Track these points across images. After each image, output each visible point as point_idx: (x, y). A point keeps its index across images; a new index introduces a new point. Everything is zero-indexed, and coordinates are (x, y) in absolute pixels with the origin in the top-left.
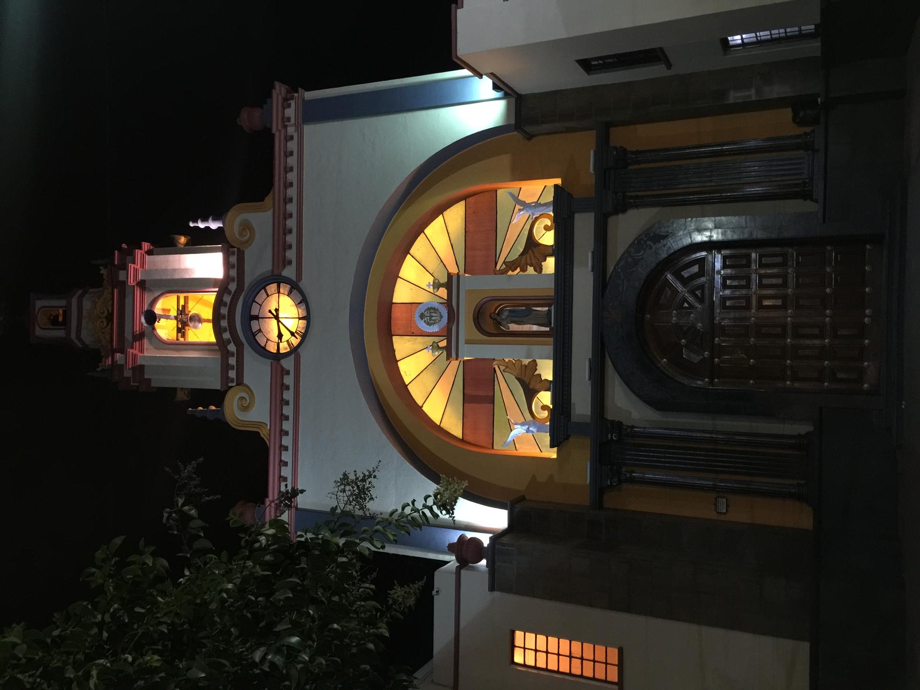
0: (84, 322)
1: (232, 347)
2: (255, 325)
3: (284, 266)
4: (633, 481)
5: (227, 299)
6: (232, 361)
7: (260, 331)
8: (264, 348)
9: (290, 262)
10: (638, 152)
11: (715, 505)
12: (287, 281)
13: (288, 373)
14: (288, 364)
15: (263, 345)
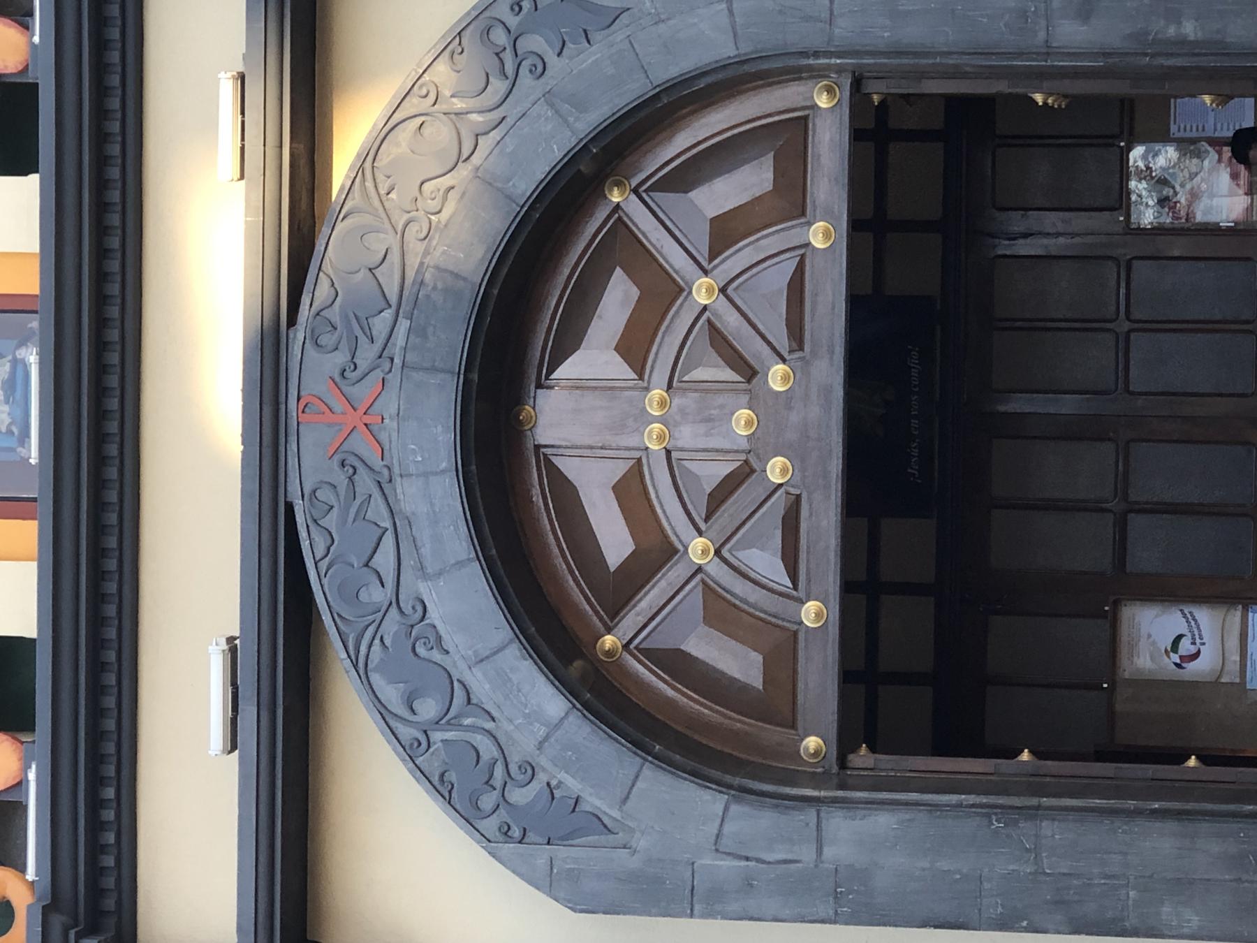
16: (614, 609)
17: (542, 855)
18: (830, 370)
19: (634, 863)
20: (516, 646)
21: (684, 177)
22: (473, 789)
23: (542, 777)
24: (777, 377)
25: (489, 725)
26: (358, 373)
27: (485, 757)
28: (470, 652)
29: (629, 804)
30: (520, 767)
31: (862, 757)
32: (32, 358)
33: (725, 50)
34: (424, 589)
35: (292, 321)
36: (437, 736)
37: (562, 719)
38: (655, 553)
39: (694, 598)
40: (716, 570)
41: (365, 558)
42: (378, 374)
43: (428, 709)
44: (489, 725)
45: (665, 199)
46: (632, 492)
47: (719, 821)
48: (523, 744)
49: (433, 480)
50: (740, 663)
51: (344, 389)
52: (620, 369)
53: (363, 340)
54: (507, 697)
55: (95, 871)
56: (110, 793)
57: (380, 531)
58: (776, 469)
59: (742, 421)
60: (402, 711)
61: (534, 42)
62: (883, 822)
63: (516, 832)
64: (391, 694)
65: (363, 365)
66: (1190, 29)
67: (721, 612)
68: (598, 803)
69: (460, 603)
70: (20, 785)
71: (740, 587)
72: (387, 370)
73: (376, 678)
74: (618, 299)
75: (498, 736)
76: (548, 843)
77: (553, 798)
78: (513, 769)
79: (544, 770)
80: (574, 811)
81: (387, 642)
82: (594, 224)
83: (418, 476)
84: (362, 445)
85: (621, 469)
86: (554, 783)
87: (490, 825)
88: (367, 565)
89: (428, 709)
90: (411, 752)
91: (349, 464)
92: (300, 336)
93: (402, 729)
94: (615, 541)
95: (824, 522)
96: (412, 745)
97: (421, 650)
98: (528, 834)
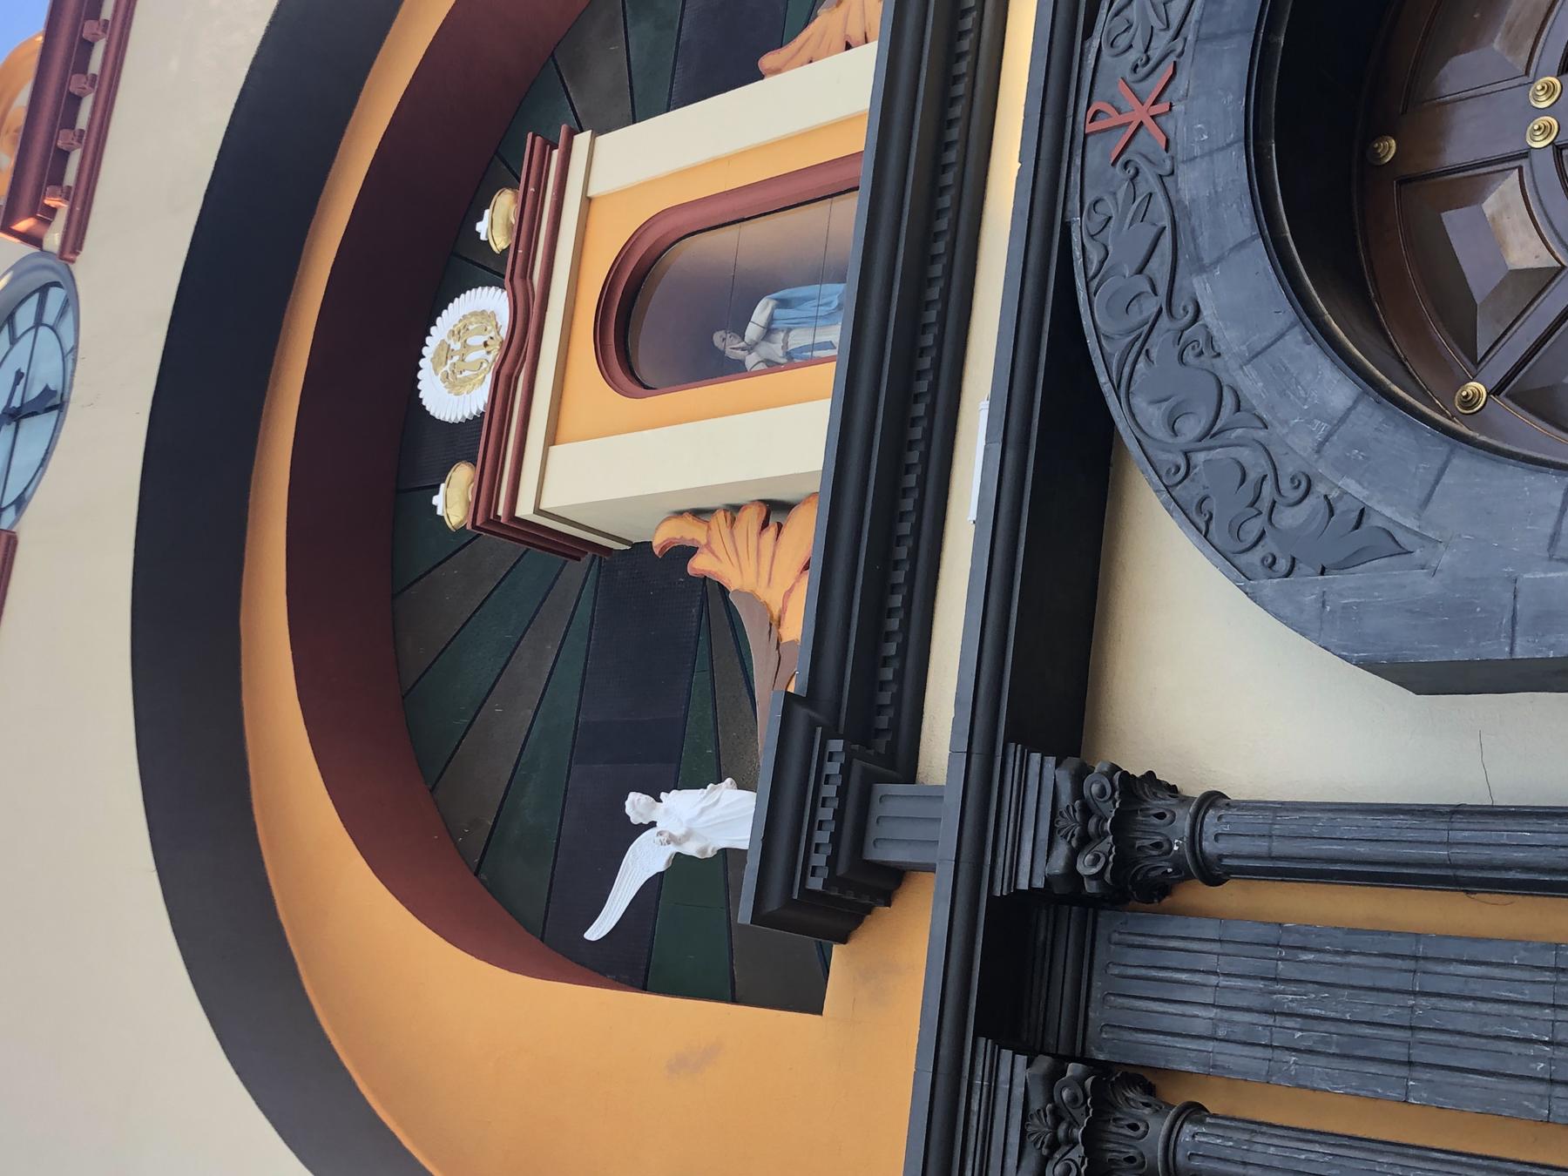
17: (1309, 589)
19: (1428, 586)
20: (1297, 335)
23: (1320, 489)
25: (1261, 434)
26: (1151, 63)
27: (1253, 476)
28: (1244, 348)
29: (1432, 506)
30: (1292, 480)
34: (1200, 287)
35: (1088, 34)
36: (1199, 458)
37: (1350, 410)
41: (1136, 266)
42: (1172, 58)
43: (1191, 428)
44: (1261, 434)
47: (1555, 515)
48: (1298, 444)
49: (1218, 157)
51: (1137, 87)
53: (1158, 25)
54: (1283, 394)
56: (897, 601)
57: (1155, 230)
60: (1161, 433)
63: (1283, 565)
64: (1152, 416)
65: (1155, 54)
68: (1388, 512)
69: (1238, 291)
72: (1179, 50)
73: (1139, 402)
75: (1271, 449)
76: (1322, 573)
77: (1332, 513)
78: (1285, 485)
79: (1322, 478)
80: (1357, 526)
81: (1154, 354)
83: (1202, 156)
86: (1334, 495)
87: (1255, 557)
88: (1140, 271)
92: (1096, 43)
93: (1160, 456)
96: (1168, 471)
97: (1189, 355)
98: (1298, 565)
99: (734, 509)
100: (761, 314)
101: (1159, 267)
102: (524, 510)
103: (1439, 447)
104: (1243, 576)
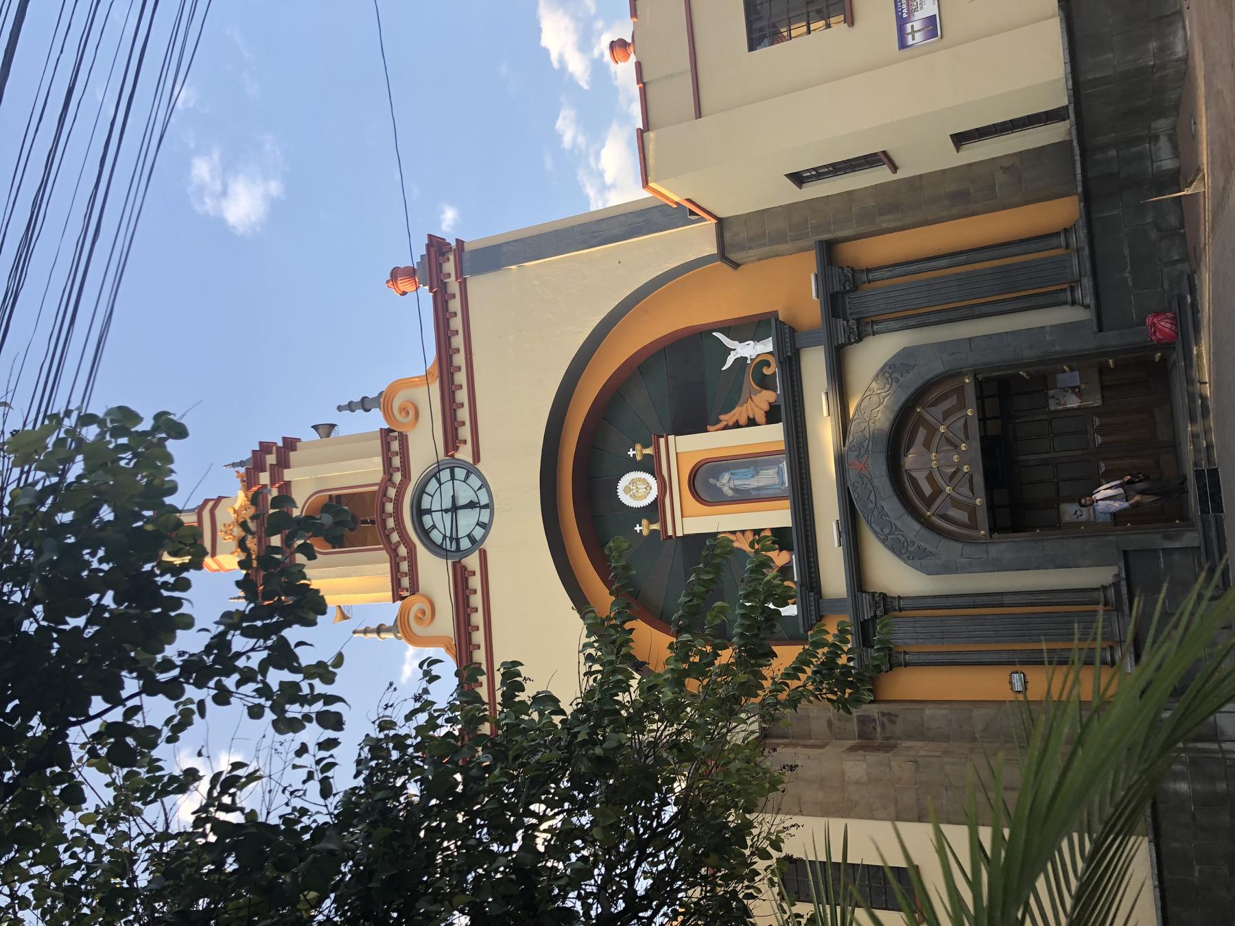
0: (220, 535)
1: (403, 551)
2: (427, 520)
3: (456, 449)
4: (906, 665)
5: (392, 492)
6: (404, 566)
7: (434, 527)
8: (440, 547)
9: (465, 442)
10: (868, 270)
11: (1011, 682)
12: (462, 464)
13: (474, 573)
14: (472, 562)
15: (439, 543)
16: (929, 506)
18: (977, 444)
21: (935, 404)
22: (900, 549)
24: (963, 447)
31: (996, 535)
32: (784, 465)
33: (942, 369)
38: (938, 491)
39: (948, 500)
40: (954, 494)
43: (887, 531)
45: (932, 409)
46: (930, 478)
50: (962, 516)
52: (925, 450)
55: (811, 578)
58: (965, 469)
59: (956, 458)
61: (895, 375)
62: (1003, 546)
64: (878, 530)
66: (1058, 348)
67: (957, 504)
69: (891, 505)
70: (791, 561)
71: (960, 498)
74: (922, 433)
82: (913, 420)
84: (864, 472)
85: (927, 473)
89: (887, 531)
90: (884, 542)
91: (860, 475)
94: (928, 491)
95: (979, 479)
99: (743, 532)
100: (726, 476)
101: (872, 497)
102: (679, 534)
103: (938, 538)
104: (904, 560)
